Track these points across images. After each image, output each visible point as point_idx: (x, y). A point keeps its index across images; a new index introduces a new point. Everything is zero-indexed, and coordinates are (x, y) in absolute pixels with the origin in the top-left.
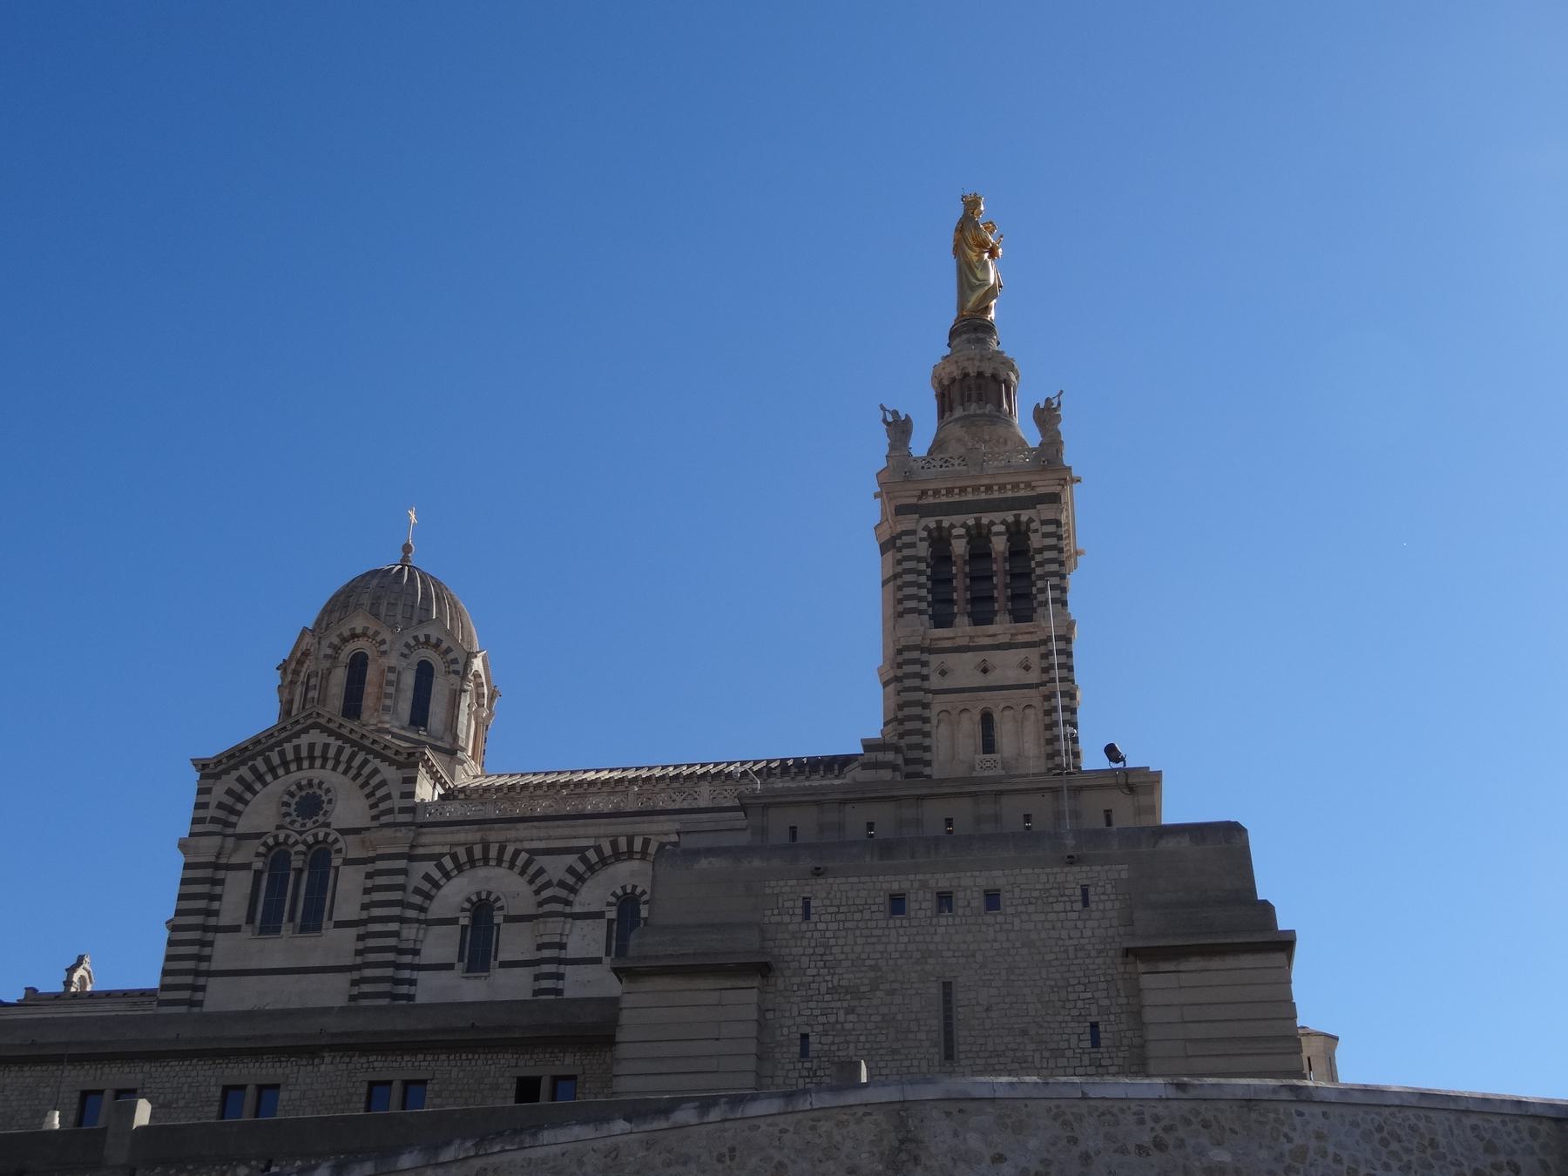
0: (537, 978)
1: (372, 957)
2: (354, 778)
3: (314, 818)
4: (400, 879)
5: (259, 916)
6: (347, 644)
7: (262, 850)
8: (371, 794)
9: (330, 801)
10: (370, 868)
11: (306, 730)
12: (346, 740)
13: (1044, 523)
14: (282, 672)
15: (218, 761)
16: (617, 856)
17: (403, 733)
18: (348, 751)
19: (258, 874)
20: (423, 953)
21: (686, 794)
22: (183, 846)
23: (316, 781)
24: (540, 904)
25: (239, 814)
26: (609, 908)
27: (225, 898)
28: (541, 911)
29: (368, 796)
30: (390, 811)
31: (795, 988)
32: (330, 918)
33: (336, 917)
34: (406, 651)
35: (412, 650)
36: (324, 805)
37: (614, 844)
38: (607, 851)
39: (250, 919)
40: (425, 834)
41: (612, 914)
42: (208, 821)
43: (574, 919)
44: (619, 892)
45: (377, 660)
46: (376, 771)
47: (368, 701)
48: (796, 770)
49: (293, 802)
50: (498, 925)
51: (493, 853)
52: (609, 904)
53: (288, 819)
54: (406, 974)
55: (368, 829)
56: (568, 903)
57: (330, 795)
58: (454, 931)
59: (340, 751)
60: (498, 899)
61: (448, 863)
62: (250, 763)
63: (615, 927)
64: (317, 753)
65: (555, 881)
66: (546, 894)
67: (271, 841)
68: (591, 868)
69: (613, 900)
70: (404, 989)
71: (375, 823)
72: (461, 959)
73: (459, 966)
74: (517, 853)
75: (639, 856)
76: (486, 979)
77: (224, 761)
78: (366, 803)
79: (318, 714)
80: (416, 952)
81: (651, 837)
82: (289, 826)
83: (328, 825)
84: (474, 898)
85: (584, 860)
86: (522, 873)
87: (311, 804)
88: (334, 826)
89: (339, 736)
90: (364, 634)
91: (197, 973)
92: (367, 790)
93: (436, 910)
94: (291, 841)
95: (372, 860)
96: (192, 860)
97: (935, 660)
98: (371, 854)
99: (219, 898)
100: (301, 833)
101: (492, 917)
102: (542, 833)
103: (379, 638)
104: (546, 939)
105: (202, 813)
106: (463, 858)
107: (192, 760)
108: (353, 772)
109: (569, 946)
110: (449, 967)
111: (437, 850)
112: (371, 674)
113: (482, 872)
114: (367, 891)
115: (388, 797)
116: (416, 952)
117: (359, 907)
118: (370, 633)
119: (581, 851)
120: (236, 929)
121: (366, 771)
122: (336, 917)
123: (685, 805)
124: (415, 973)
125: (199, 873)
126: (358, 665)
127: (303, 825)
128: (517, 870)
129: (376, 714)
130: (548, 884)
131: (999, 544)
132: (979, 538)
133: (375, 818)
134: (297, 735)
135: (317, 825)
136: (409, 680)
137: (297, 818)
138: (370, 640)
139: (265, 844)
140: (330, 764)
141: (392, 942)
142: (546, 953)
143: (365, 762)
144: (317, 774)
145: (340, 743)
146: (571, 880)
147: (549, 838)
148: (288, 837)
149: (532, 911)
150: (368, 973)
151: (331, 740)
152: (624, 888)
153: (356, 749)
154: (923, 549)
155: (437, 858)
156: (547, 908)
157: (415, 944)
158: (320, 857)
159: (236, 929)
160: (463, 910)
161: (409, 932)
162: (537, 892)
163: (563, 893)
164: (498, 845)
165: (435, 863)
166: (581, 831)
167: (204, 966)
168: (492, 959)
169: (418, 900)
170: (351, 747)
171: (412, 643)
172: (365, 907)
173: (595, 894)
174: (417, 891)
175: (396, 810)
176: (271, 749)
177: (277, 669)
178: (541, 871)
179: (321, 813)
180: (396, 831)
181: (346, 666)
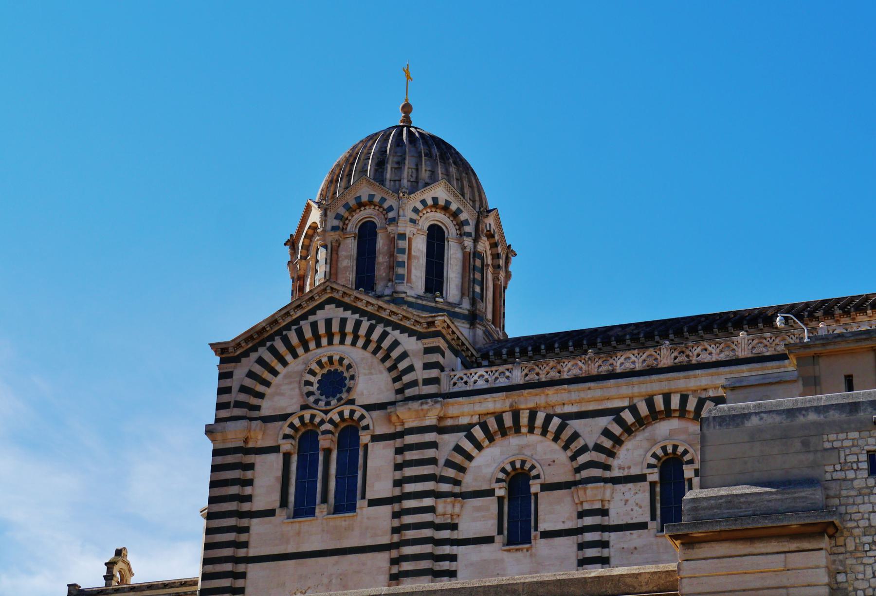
0: (581, 546)
1: (410, 534)
2: (375, 353)
3: (338, 396)
4: (430, 453)
5: (292, 498)
6: (354, 214)
7: (288, 431)
8: (393, 368)
9: (352, 377)
10: (398, 443)
11: (321, 307)
12: (363, 313)
14: (290, 248)
15: (237, 343)
16: (655, 415)
17: (420, 302)
18: (365, 325)
19: (287, 456)
20: (460, 527)
21: (722, 345)
22: (210, 431)
23: (336, 358)
24: (578, 470)
25: (261, 396)
26: (650, 470)
27: (256, 482)
28: (578, 477)
29: (390, 369)
31: (867, 547)
32: (363, 497)
33: (370, 495)
34: (414, 216)
35: (421, 214)
36: (347, 382)
37: (650, 402)
38: (643, 410)
39: (284, 503)
40: (453, 404)
41: (654, 476)
42: (232, 405)
43: (614, 484)
44: (660, 453)
45: (386, 228)
47: (381, 271)
48: (841, 312)
49: (314, 380)
50: (536, 495)
51: (524, 420)
52: (650, 466)
53: (312, 399)
54: (447, 550)
55: (393, 403)
56: (607, 467)
57: (351, 371)
58: (491, 504)
59: (358, 324)
60: (533, 467)
61: (478, 432)
62: (268, 344)
63: (658, 489)
64: (335, 328)
65: (591, 445)
66: (582, 459)
67: (297, 422)
68: (628, 430)
69: (653, 461)
70: (445, 565)
71: (399, 397)
72: (500, 532)
73: (499, 539)
74: (548, 419)
75: (677, 414)
76: (527, 551)
77: (243, 344)
79: (332, 289)
80: (454, 527)
81: (689, 393)
82: (314, 406)
83: (352, 402)
84: (509, 468)
85: (620, 422)
86: (556, 439)
88: (360, 401)
89: (355, 310)
90: (371, 202)
91: (237, 560)
92: (388, 364)
93: (470, 482)
94: (317, 420)
95: (401, 435)
96: (220, 446)
98: (399, 429)
99: (250, 482)
100: (326, 412)
101: (529, 487)
102: (574, 396)
103: (386, 205)
104: (587, 506)
105: (225, 398)
106: (493, 425)
107: (211, 345)
108: (372, 346)
109: (612, 513)
110: (489, 540)
111: (464, 421)
112: (381, 242)
113: (514, 441)
114: (398, 467)
115: (411, 369)
116: (454, 527)
117: (391, 484)
118: (377, 199)
119: (615, 413)
120: (271, 513)
121: (386, 344)
122: (370, 495)
123: (722, 357)
124: (455, 547)
125: (230, 459)
127: (328, 404)
128: (550, 436)
129: (390, 284)
130: (584, 449)
133: (399, 391)
134: (313, 312)
135: (342, 402)
136: (420, 245)
137: (321, 397)
138: (377, 208)
139: (292, 426)
140: (349, 339)
141: (427, 517)
142: (588, 521)
143: (385, 335)
144: (337, 350)
145: (357, 316)
146: (608, 443)
147: (580, 402)
148: (313, 417)
149: (569, 477)
150: (408, 550)
151: (348, 314)
152: (664, 448)
153: (374, 322)
155: (467, 429)
156: (585, 474)
157: (452, 519)
159: (271, 513)
160: (499, 481)
161: (444, 507)
162: (573, 458)
163: (601, 457)
164: (528, 411)
165: (464, 433)
166: (613, 392)
167: (242, 553)
168: (532, 530)
169: (451, 473)
170: (368, 320)
171: (420, 207)
172: (398, 483)
174: (449, 464)
175: (420, 382)
176: (288, 327)
177: (285, 244)
178: (575, 436)
179: (344, 390)
180: (422, 404)
181: (355, 238)
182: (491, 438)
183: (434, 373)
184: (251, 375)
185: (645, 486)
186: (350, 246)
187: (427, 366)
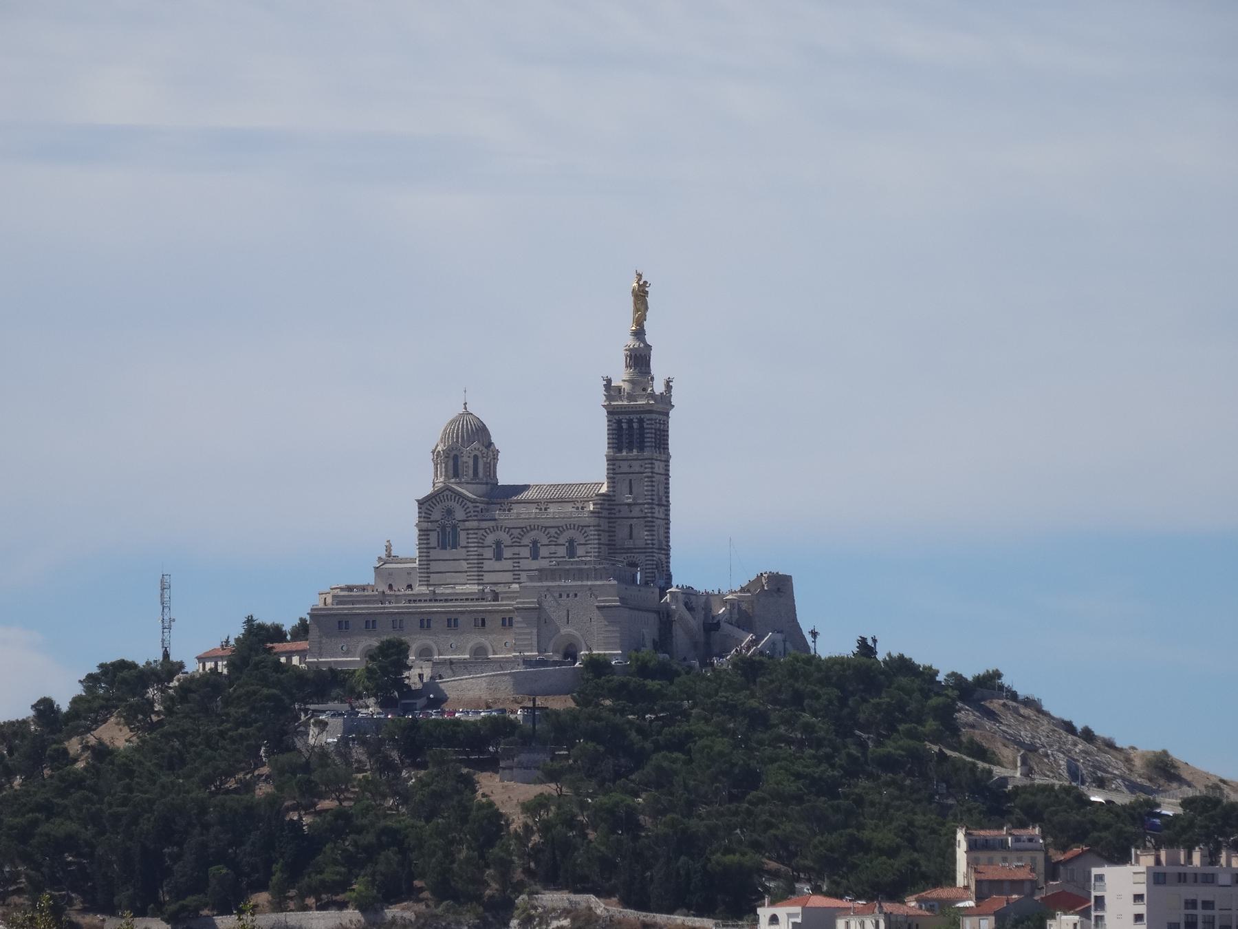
8: (465, 510)
11: (445, 491)
13: (648, 420)
22: (417, 525)
30: (471, 516)
39: (438, 546)
46: (466, 504)
54: (481, 561)
66: (514, 540)
78: (464, 513)
80: (482, 555)
87: (449, 512)
97: (617, 462)
109: (521, 554)
110: (491, 559)
115: (470, 512)
116: (482, 555)
126: (456, 458)
131: (635, 425)
132: (630, 422)
136: (471, 463)
154: (615, 426)
158: (454, 527)
159: (435, 548)
161: (480, 550)
163: (518, 540)
169: (481, 541)
173: (526, 541)
182: (491, 532)
183: (476, 513)
184: (427, 509)
185: (529, 548)
186: (451, 463)
187: (474, 512)
